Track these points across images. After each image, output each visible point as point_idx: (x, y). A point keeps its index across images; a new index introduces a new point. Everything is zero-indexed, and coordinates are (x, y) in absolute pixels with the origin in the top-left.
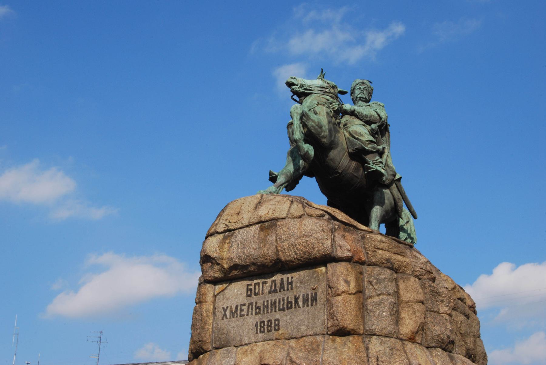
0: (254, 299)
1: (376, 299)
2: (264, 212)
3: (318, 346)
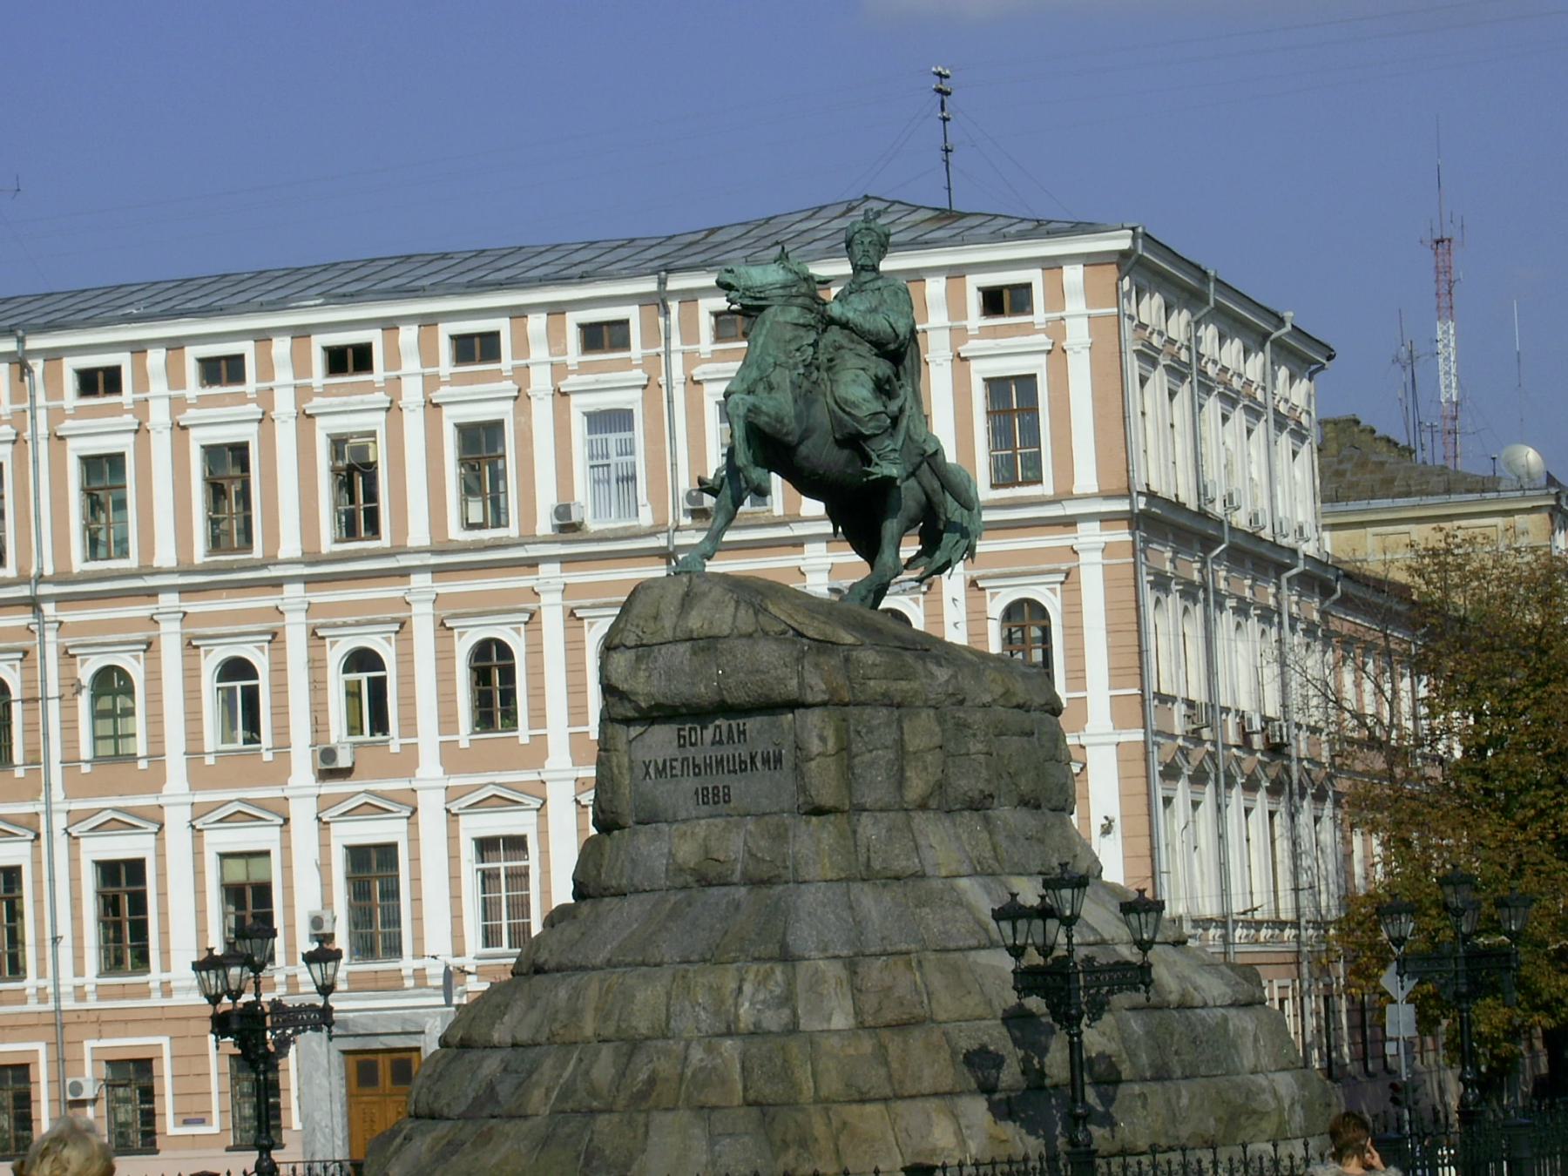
0: (690, 752)
1: (867, 757)
2: (695, 622)
3: (786, 830)
